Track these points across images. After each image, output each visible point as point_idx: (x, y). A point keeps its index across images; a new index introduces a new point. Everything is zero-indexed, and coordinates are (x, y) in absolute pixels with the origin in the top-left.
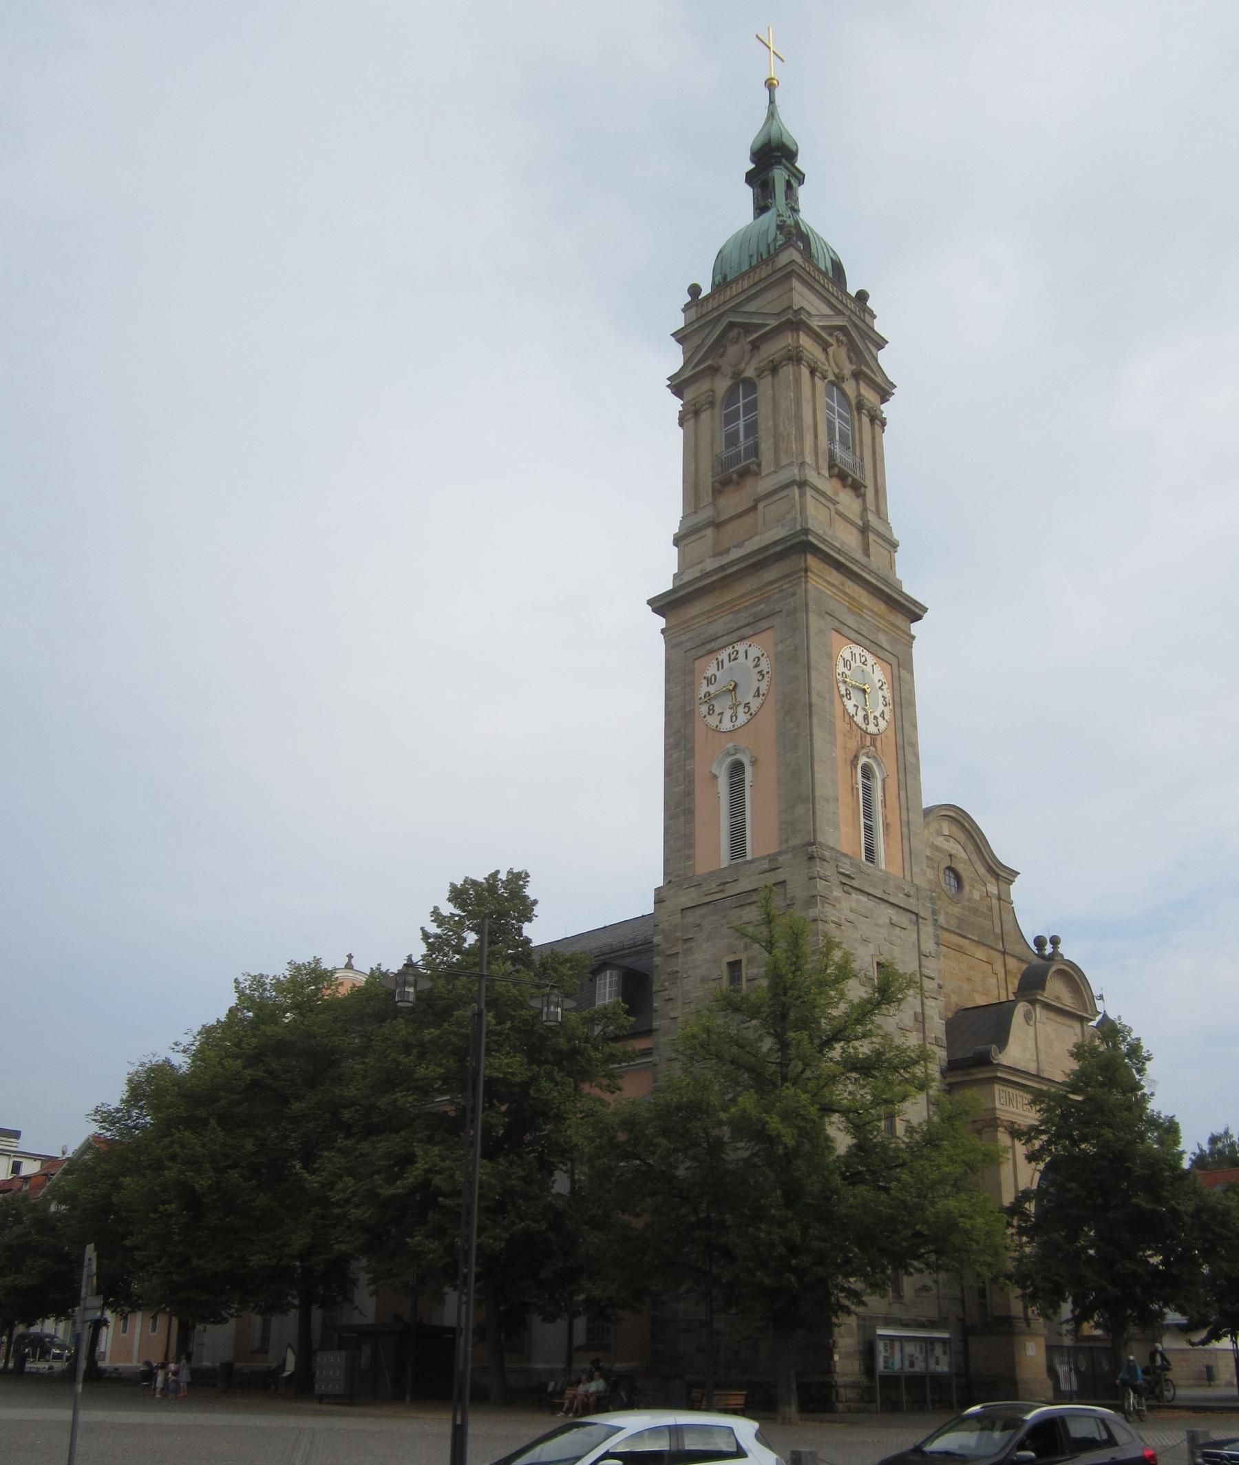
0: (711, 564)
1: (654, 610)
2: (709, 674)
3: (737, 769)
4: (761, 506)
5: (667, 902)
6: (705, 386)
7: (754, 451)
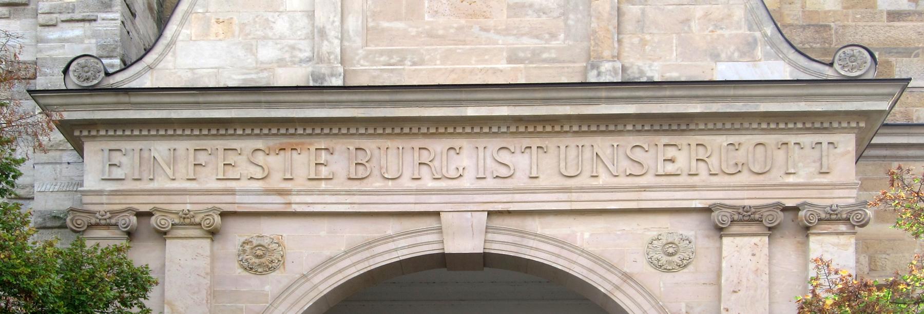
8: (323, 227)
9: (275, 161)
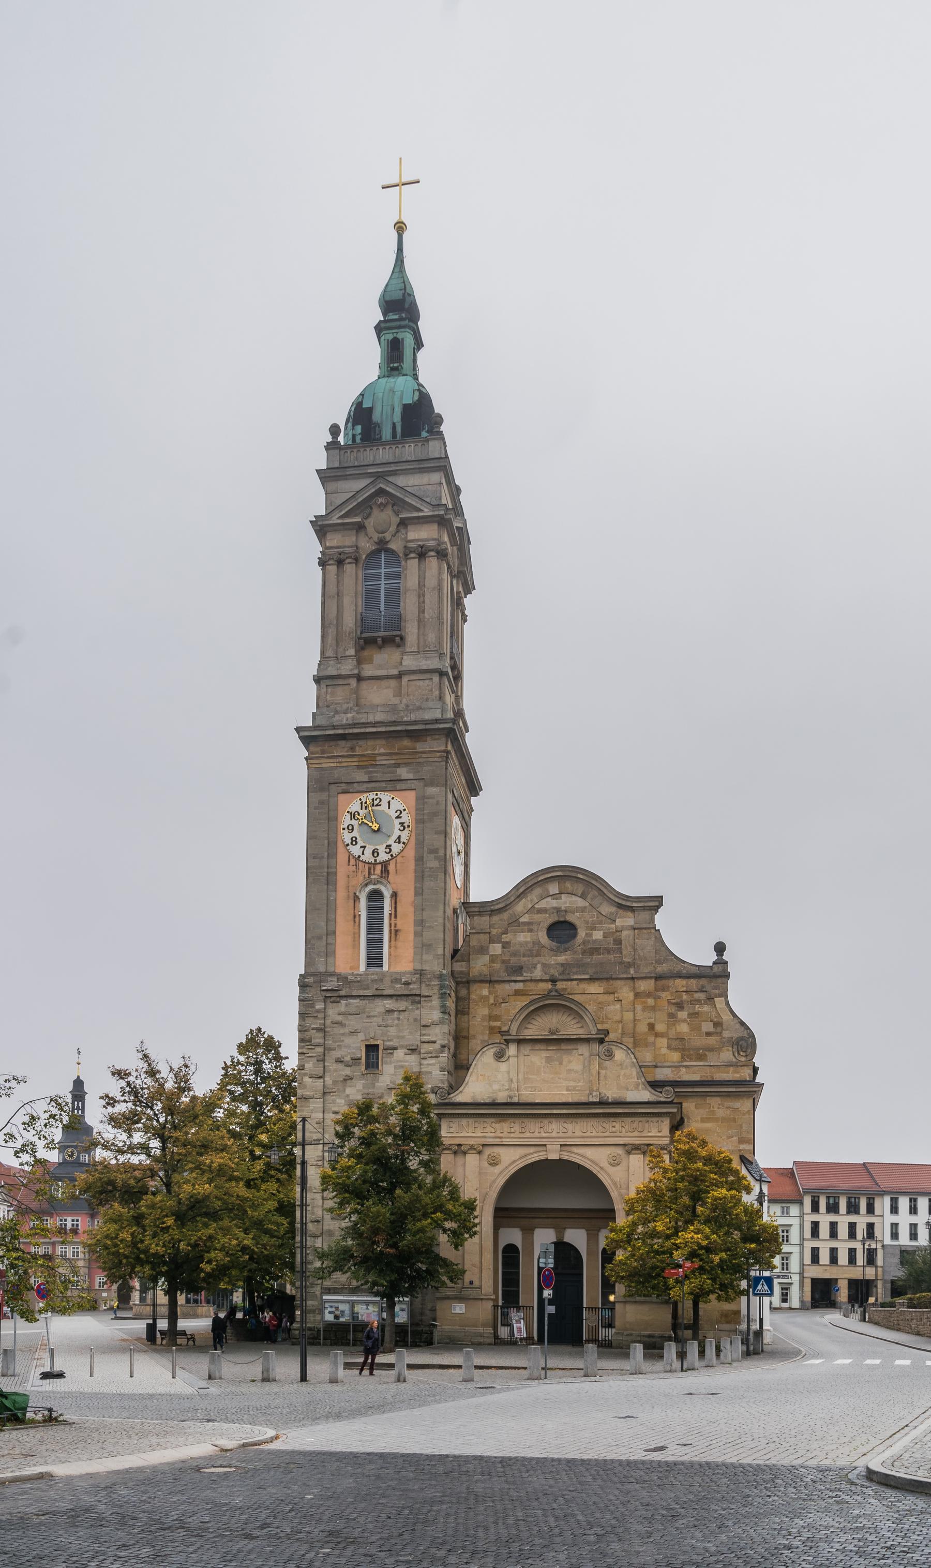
1: (300, 738)
2: (353, 810)
3: (375, 896)
4: (405, 679)
7: (397, 622)
8: (512, 1149)
9: (498, 1126)
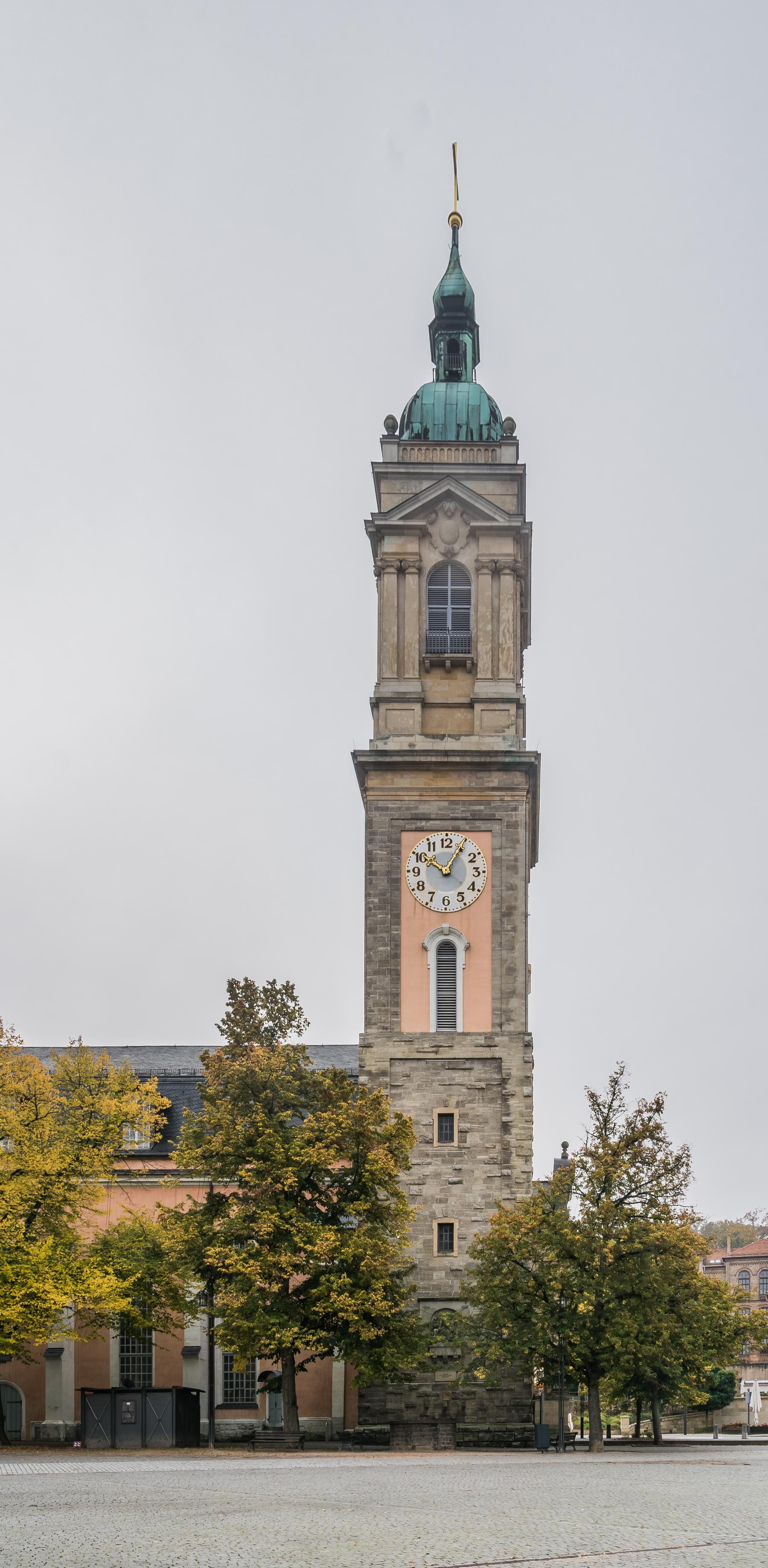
0: (422, 743)
2: (419, 851)
3: (446, 949)
4: (478, 707)
5: (374, 1049)
6: (412, 546)
